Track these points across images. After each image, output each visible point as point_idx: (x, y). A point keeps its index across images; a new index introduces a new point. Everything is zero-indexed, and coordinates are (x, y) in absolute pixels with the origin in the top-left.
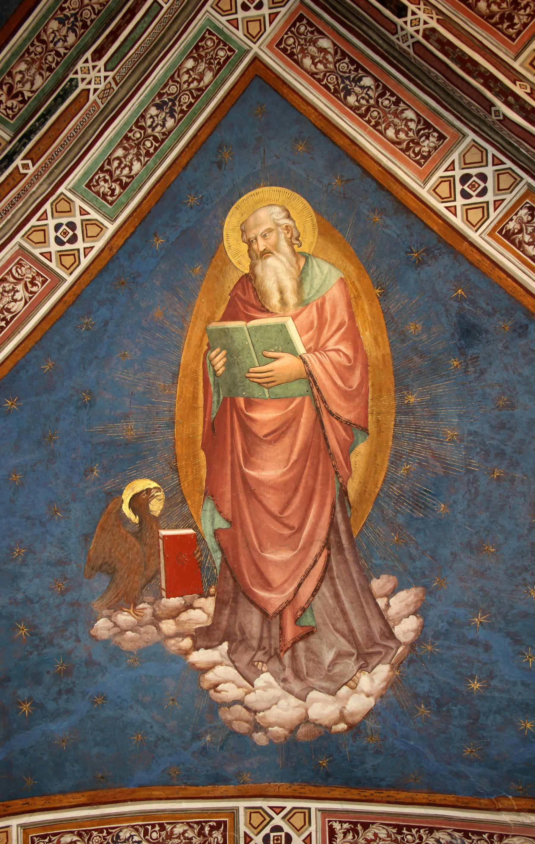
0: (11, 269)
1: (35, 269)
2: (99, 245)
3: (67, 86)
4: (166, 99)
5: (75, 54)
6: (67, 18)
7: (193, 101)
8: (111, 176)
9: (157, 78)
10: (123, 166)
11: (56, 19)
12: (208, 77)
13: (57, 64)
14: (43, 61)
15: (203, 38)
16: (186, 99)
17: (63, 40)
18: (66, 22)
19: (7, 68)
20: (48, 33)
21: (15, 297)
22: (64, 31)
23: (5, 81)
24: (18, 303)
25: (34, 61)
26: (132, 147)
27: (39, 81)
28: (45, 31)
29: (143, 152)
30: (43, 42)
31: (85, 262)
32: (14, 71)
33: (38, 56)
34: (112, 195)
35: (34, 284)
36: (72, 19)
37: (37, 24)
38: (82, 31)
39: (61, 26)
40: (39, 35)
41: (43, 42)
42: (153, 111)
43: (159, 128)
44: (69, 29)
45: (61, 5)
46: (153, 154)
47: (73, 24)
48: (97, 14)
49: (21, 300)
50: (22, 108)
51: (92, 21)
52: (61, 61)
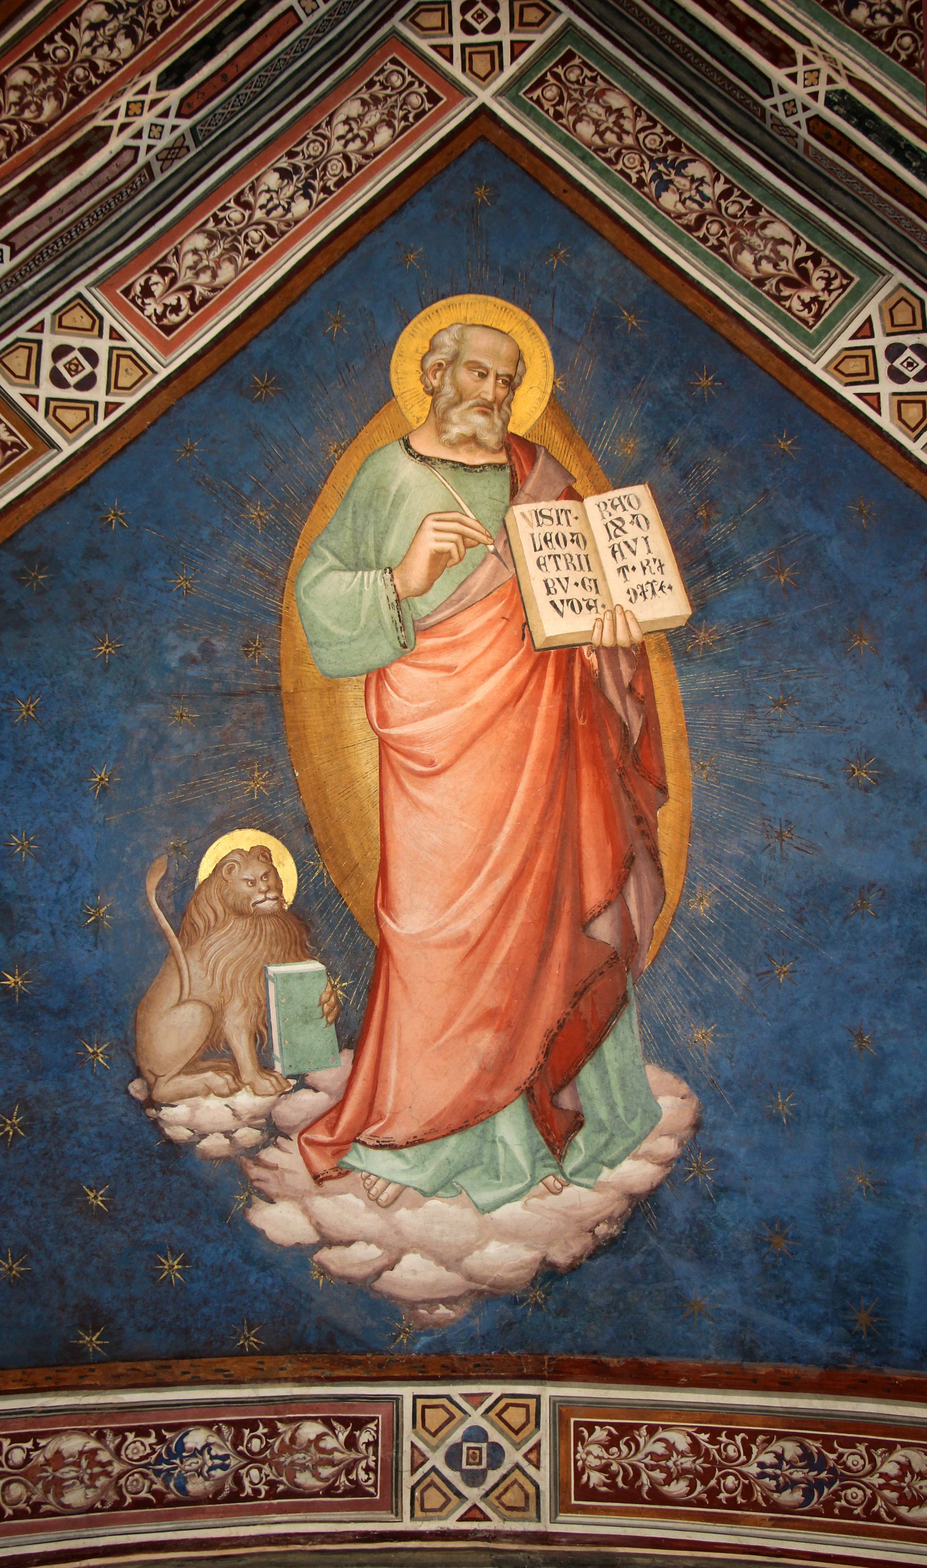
5: (729, 165)
6: (658, 175)
9: (792, 10)
11: (658, 196)
13: (744, 196)
14: (738, 221)
17: (701, 185)
18: (665, 177)
19: (747, 286)
20: (683, 210)
22: (682, 183)
25: (736, 238)
27: (777, 230)
28: (679, 216)
30: (700, 220)
32: (755, 274)
33: (728, 230)
36: (661, 167)
37: (665, 230)
38: (684, 150)
39: (672, 187)
40: (687, 227)
41: (700, 220)
45: (634, 185)
47: (672, 165)
48: (655, 123)
50: (829, 261)
51: (667, 132)
52: (739, 189)
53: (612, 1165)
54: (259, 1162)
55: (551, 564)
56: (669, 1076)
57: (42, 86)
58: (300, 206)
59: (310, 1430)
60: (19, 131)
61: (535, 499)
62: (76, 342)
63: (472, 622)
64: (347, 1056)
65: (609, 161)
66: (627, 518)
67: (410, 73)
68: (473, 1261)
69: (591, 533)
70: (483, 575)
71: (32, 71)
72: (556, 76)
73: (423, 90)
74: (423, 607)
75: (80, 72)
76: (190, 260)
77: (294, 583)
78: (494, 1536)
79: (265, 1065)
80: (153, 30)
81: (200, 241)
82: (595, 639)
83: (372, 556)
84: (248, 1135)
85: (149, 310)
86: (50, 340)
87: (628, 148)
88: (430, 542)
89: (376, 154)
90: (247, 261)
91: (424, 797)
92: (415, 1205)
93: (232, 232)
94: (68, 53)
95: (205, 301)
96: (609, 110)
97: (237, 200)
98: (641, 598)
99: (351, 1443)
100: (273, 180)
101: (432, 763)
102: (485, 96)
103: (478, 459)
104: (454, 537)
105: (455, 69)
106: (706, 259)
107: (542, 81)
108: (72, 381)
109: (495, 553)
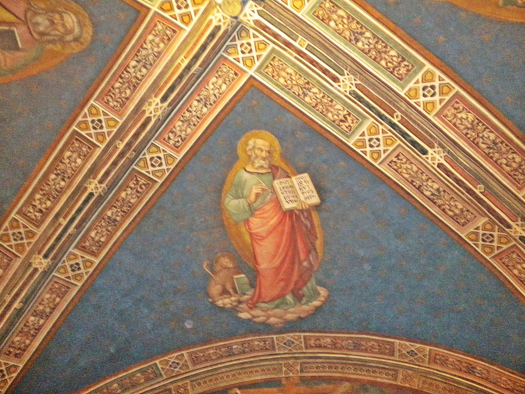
0: (448, 120)
1: (449, 108)
2: (438, 73)
3: (354, 96)
4: (354, 37)
7: (356, 21)
8: (396, 67)
9: (340, 43)
10: (391, 61)
12: (341, 12)
13: (328, 97)
14: (327, 105)
15: (318, 17)
16: (354, 25)
21: (465, 118)
22: (310, 94)
23: (338, 124)
24: (469, 117)
25: (327, 110)
26: (381, 56)
29: (384, 49)
30: (317, 105)
31: (447, 80)
34: (408, 66)
35: (459, 108)
36: (304, 90)
38: (310, 84)
40: (313, 107)
41: (317, 105)
42: (360, 44)
43: (371, 41)
44: (310, 91)
46: (386, 44)
49: (467, 115)
53: (311, 302)
54: (238, 307)
55: (285, 193)
56: (322, 288)
57: (124, 86)
58: (205, 110)
59: (256, 343)
60: (122, 101)
61: (279, 178)
62: (155, 155)
63: (268, 207)
64: (253, 290)
65: (289, 89)
66: (303, 181)
67: (228, 67)
68: (285, 317)
69: (294, 184)
70: (269, 197)
71: (120, 83)
72: (271, 64)
73: (233, 72)
74: (255, 205)
75: (134, 80)
76: (178, 128)
77: (223, 204)
78: (295, 353)
79: (236, 292)
80: (151, 64)
81: (180, 123)
82: (298, 208)
83: (241, 195)
84: (235, 304)
85: (171, 143)
86: (148, 157)
87: (295, 85)
88: (255, 191)
89: (224, 92)
90: (194, 127)
91: (262, 243)
92: (271, 311)
93: (188, 120)
94: (129, 76)
95: (185, 139)
96: (288, 73)
97: (188, 110)
98: (308, 199)
99: (265, 344)
100: (195, 103)
101: (262, 236)
102: (251, 72)
103: (264, 171)
104: (261, 189)
105: (241, 65)
106: (318, 115)
107: (267, 67)
108: (156, 165)
109: (271, 192)
